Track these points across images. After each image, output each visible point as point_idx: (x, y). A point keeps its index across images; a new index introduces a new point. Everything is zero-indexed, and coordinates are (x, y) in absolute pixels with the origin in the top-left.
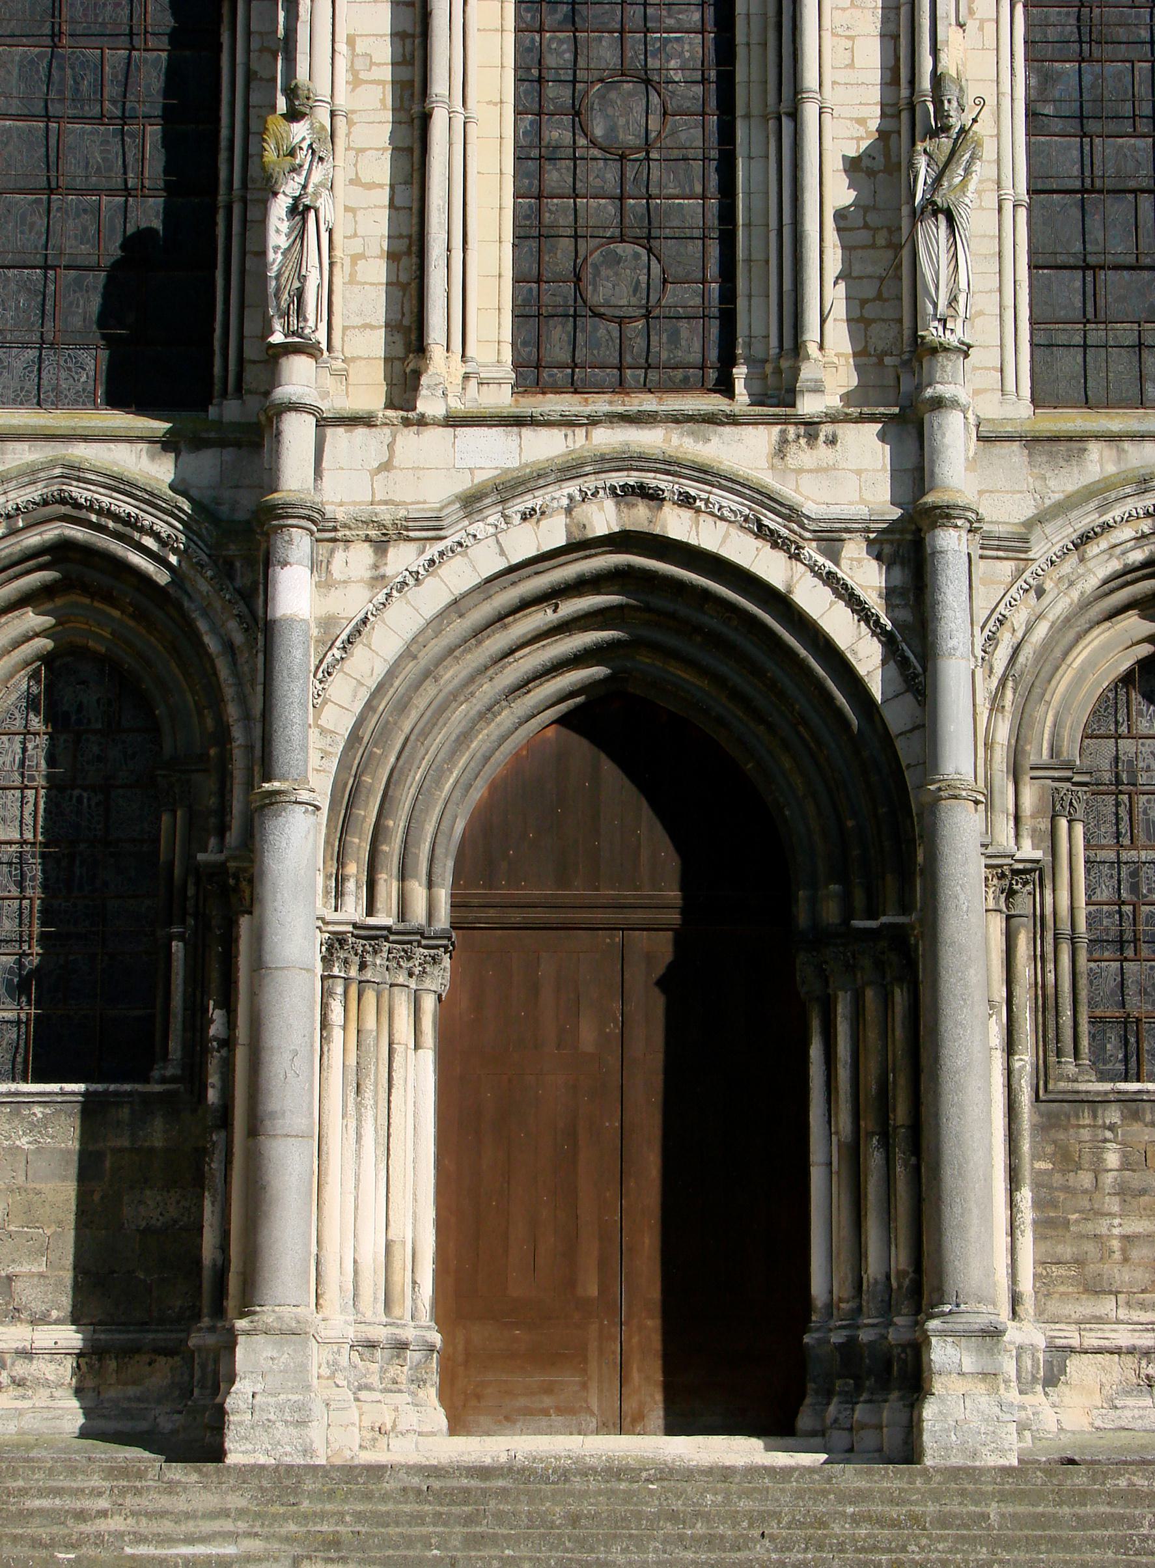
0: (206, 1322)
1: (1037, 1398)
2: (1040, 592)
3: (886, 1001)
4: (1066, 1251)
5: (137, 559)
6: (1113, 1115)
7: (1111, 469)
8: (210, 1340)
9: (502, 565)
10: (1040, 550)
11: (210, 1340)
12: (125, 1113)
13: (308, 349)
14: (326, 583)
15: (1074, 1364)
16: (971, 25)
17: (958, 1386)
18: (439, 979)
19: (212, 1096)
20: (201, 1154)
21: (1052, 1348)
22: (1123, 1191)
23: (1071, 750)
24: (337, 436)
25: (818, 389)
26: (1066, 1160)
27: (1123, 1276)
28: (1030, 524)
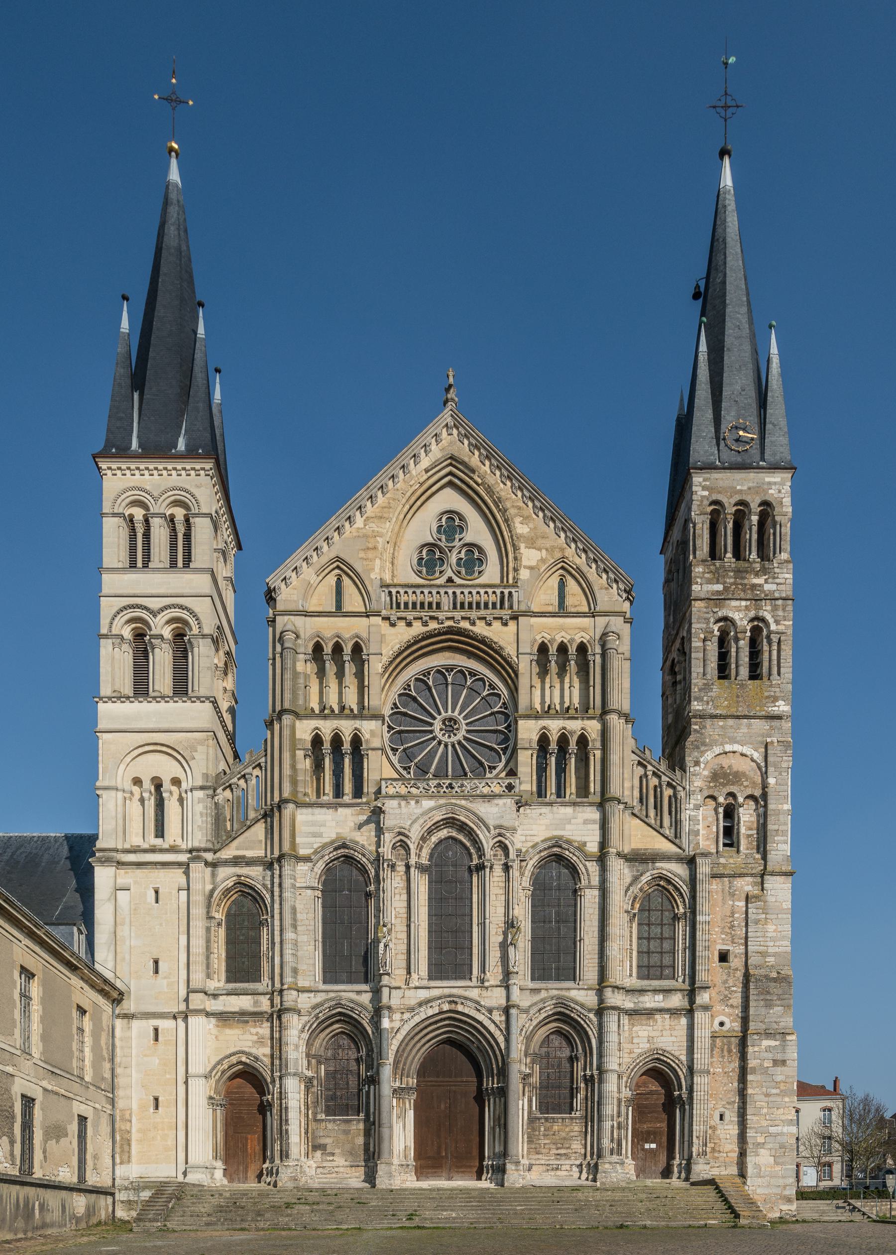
0: (371, 1161)
1: (527, 1173)
2: (531, 1020)
3: (500, 1101)
4: (533, 1146)
5: (354, 1015)
6: (543, 1121)
7: (546, 995)
8: (372, 1164)
9: (426, 1017)
10: (532, 1012)
11: (372, 1164)
12: (355, 1122)
13: (388, 974)
14: (392, 1021)
15: (534, 1167)
16: (520, 904)
17: (512, 1172)
18: (414, 1097)
19: (371, 1119)
20: (370, 1130)
21: (530, 1164)
22: (544, 1135)
23: (537, 1051)
24: (393, 991)
25: (488, 981)
26: (534, 1130)
27: (544, 1151)
28: (530, 1007)
